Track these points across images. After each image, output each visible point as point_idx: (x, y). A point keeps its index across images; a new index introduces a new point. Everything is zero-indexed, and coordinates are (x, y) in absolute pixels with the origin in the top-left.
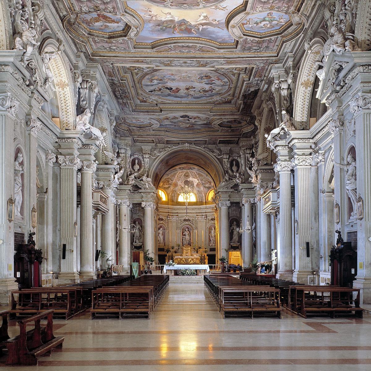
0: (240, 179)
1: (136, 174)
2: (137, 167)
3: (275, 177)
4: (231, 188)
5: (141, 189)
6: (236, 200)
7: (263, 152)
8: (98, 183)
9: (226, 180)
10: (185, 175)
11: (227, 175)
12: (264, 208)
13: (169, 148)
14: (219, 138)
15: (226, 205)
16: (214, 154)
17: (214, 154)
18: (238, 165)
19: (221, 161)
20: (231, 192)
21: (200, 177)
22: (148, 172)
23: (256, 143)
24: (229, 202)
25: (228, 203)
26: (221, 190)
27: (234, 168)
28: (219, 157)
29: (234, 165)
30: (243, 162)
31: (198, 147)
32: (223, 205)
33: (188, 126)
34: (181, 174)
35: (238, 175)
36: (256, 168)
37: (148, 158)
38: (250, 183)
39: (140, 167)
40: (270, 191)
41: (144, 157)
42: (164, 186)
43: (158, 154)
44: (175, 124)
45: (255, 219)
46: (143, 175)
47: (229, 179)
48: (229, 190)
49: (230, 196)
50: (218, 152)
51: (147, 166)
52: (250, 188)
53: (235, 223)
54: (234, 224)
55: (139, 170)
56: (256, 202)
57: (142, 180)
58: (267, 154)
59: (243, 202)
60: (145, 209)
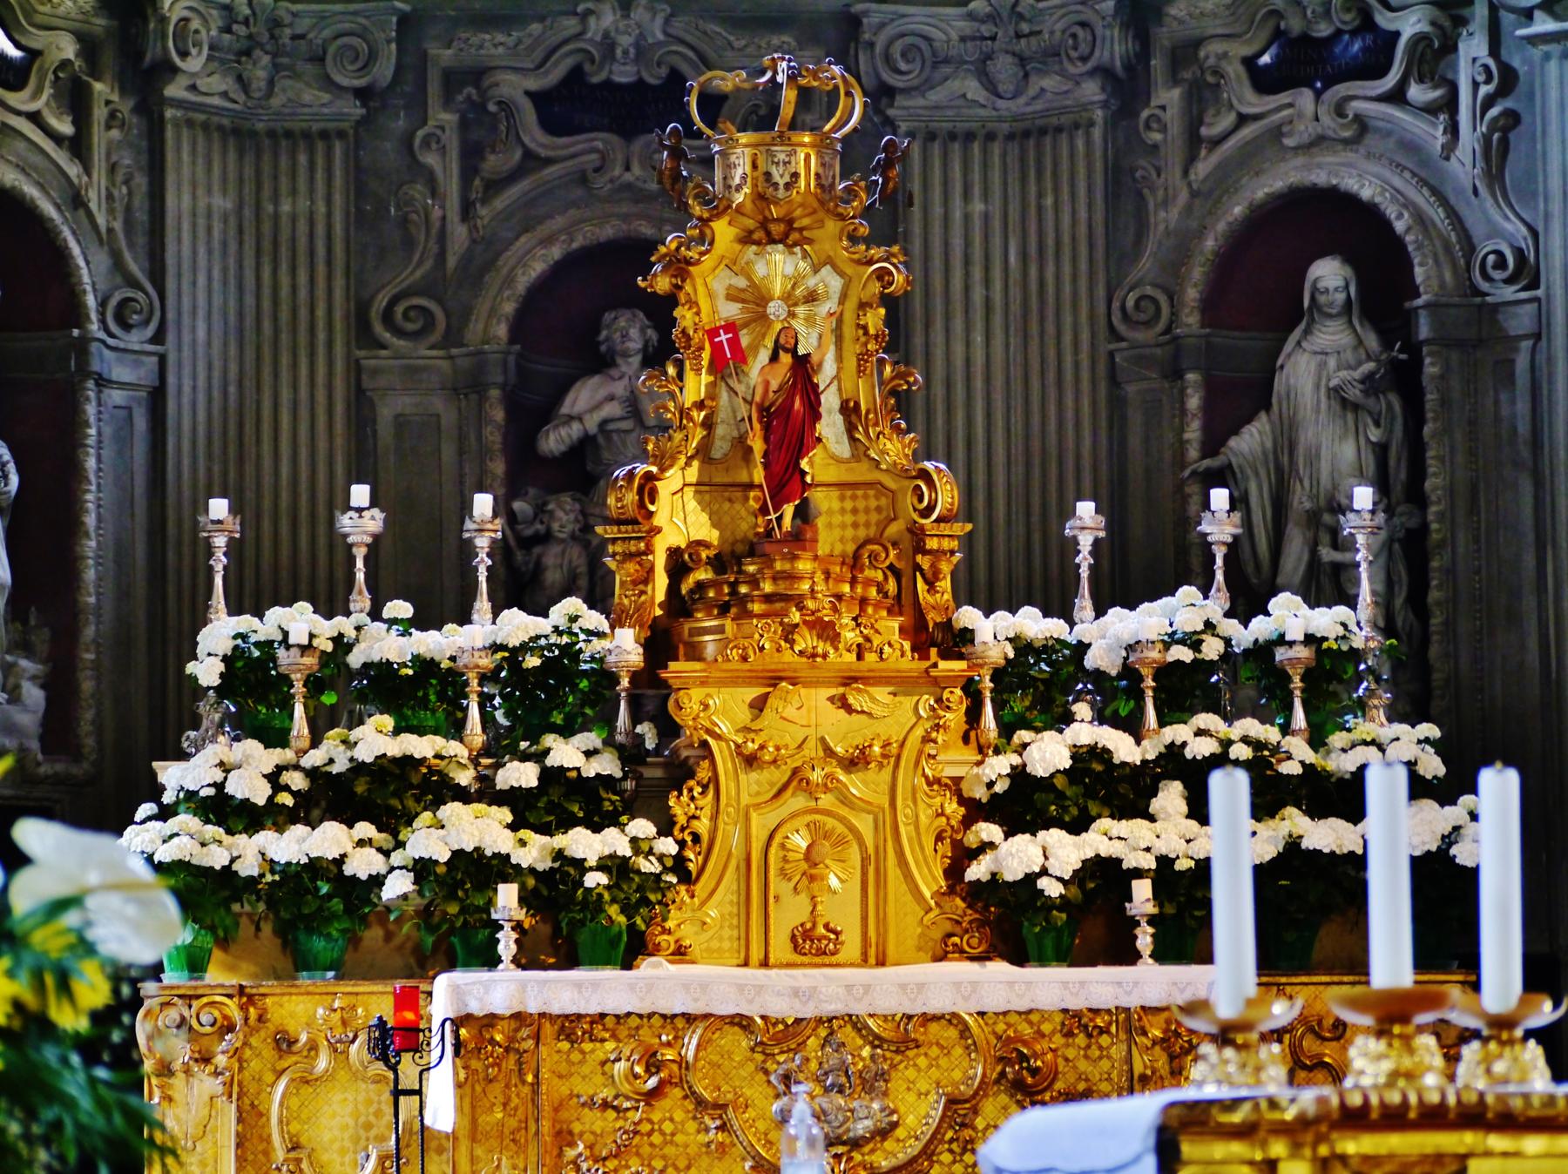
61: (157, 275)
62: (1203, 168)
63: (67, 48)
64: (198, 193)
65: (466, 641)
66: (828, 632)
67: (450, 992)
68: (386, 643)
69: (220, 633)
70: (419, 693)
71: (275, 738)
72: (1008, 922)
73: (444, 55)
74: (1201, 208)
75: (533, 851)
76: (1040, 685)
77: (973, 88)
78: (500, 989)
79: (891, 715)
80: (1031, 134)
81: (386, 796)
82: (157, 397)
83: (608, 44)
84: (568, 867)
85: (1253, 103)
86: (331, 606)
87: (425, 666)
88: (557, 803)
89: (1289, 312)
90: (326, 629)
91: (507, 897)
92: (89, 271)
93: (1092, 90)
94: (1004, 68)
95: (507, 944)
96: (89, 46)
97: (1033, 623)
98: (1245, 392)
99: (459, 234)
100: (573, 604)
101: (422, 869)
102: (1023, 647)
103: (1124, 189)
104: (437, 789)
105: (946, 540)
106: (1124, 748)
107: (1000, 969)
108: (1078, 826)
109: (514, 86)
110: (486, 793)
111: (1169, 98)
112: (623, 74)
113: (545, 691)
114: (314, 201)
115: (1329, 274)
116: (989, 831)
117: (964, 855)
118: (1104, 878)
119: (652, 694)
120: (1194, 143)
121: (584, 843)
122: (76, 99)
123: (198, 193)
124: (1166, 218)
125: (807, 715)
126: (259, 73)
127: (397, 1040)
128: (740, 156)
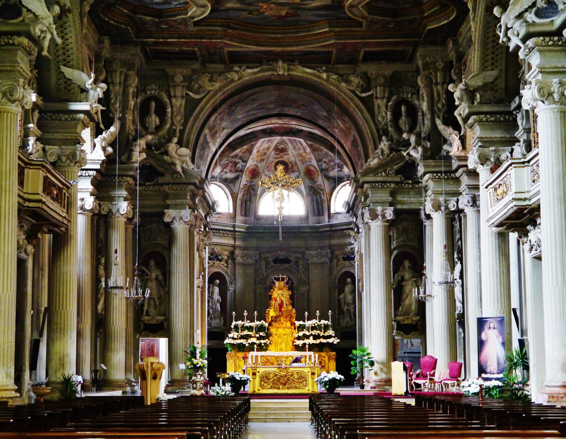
0: (420, 149)
1: (150, 137)
2: (154, 120)
3: (520, 134)
4: (397, 173)
5: (162, 175)
6: (408, 201)
7: (483, 68)
8: (44, 149)
10: (276, 149)
11: (384, 138)
12: (491, 215)
13: (236, 72)
14: (365, 44)
15: (384, 216)
18: (413, 112)
19: (368, 103)
20: (397, 183)
21: (316, 153)
22: (182, 132)
23: (461, 57)
24: (392, 208)
25: (390, 213)
26: (371, 178)
27: (403, 121)
28: (364, 95)
30: (425, 106)
31: (308, 70)
32: (374, 216)
33: (283, 13)
34: (265, 146)
35: (413, 139)
36: (467, 111)
38: (448, 158)
40: (511, 165)
41: (172, 94)
42: (225, 176)
44: (252, 8)
45: (460, 252)
46: (169, 140)
47: (391, 149)
48: (390, 179)
49: (393, 194)
51: (179, 118)
52: (446, 172)
53: (407, 264)
54: (404, 267)
55: (158, 128)
56: (461, 206)
57: (166, 153)
58: (495, 73)
59: (429, 208)
61: (235, 279)
62: (338, 268)
63: (226, 257)
64: (239, 271)
65: (252, 324)
66: (282, 324)
67: (251, 353)
68: (247, 324)
69: (234, 323)
70: (250, 328)
71: (238, 332)
72: (297, 348)
73: (263, 256)
74: (337, 273)
75: (258, 342)
76: (301, 328)
77: (316, 259)
78: (254, 353)
79: (288, 331)
80: (323, 264)
81: (246, 337)
82: (235, 291)
83: (280, 255)
84: (261, 343)
85: (343, 262)
86: (243, 321)
87: (250, 326)
88: (259, 338)
89: (346, 283)
90: (242, 323)
91: (255, 346)
92: (228, 279)
93: (328, 260)
94: (319, 257)
95: (255, 350)
96: (228, 257)
97: (301, 323)
98: (342, 291)
99: (265, 274)
100: (262, 321)
101: (249, 343)
102: (300, 325)
103: (331, 269)
104: (251, 336)
105: (294, 315)
106: (308, 333)
107: (296, 352)
108: (303, 340)
109: (271, 259)
110: (255, 337)
111: (335, 261)
112: (281, 258)
113: (261, 328)
114: (250, 271)
115: (349, 280)
116: (296, 340)
117: (294, 342)
118: (304, 344)
119: (268, 329)
120: (337, 266)
121: (262, 341)
122: (227, 262)
123: (239, 271)
124: (335, 273)
125: (281, 331)
126: (245, 258)
127: (245, 358)
128: (277, 283)
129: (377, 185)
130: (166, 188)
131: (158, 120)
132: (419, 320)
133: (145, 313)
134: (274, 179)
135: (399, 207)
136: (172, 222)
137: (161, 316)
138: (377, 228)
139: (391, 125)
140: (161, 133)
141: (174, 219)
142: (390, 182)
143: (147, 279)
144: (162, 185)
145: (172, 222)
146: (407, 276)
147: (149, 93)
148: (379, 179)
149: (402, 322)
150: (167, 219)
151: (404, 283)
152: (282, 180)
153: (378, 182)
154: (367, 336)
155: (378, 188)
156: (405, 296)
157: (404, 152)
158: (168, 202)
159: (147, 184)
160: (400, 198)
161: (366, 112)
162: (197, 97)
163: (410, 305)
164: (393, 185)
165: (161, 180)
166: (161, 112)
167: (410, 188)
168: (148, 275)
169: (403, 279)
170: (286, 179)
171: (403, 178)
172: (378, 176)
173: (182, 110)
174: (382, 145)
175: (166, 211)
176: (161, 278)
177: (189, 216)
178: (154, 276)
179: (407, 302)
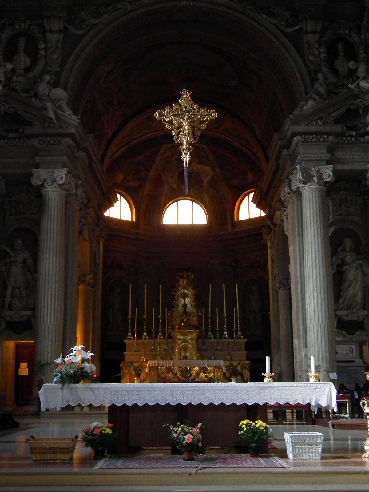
2: (23, 60)
4: (337, 121)
5: (30, 124)
9: (318, 93)
11: (320, 76)
15: (320, 178)
16: (275, 21)
17: (275, 21)
20: (337, 135)
24: (331, 166)
25: (328, 173)
26: (303, 128)
28: (289, 30)
29: (341, 53)
32: (307, 179)
37: (60, 31)
39: (34, 61)
43: (94, 21)
47: (329, 92)
48: (328, 129)
49: (331, 150)
50: (286, 14)
51: (55, 56)
53: (348, 243)
55: (28, 70)
57: (36, 96)
60: (43, 191)
129: (311, 137)
130: (35, 142)
131: (28, 60)
132: (366, 316)
133: (6, 306)
134: (177, 109)
135: (339, 167)
136: (42, 185)
137: (26, 309)
138: (310, 195)
139: (325, 65)
140: (31, 75)
141: (45, 181)
142: (329, 134)
143: (11, 261)
144: (30, 137)
145: (42, 185)
146: (348, 259)
147: (17, 26)
148: (314, 129)
149: (345, 319)
150: (35, 182)
151: (345, 267)
152: (189, 112)
153: (312, 133)
154: (299, 336)
155: (312, 142)
156: (347, 284)
157: (352, 85)
158: (38, 159)
159: (10, 135)
160: (339, 154)
161: (293, 49)
162: (79, 32)
163: (354, 296)
164: (331, 138)
165: (28, 130)
166: (32, 52)
167: (352, 143)
168: (10, 257)
169: (343, 262)
170: (194, 109)
171: (345, 128)
172: (313, 125)
173: (60, 45)
174: (317, 86)
175: (34, 170)
176: (30, 261)
177: (64, 176)
178: (20, 258)
179: (351, 292)
